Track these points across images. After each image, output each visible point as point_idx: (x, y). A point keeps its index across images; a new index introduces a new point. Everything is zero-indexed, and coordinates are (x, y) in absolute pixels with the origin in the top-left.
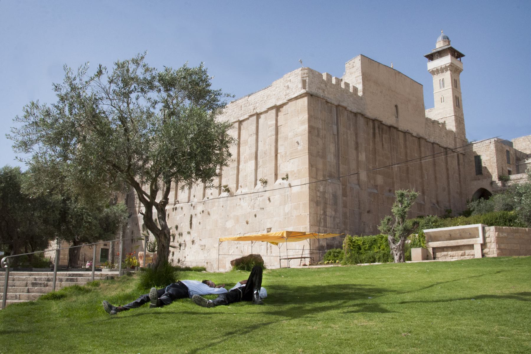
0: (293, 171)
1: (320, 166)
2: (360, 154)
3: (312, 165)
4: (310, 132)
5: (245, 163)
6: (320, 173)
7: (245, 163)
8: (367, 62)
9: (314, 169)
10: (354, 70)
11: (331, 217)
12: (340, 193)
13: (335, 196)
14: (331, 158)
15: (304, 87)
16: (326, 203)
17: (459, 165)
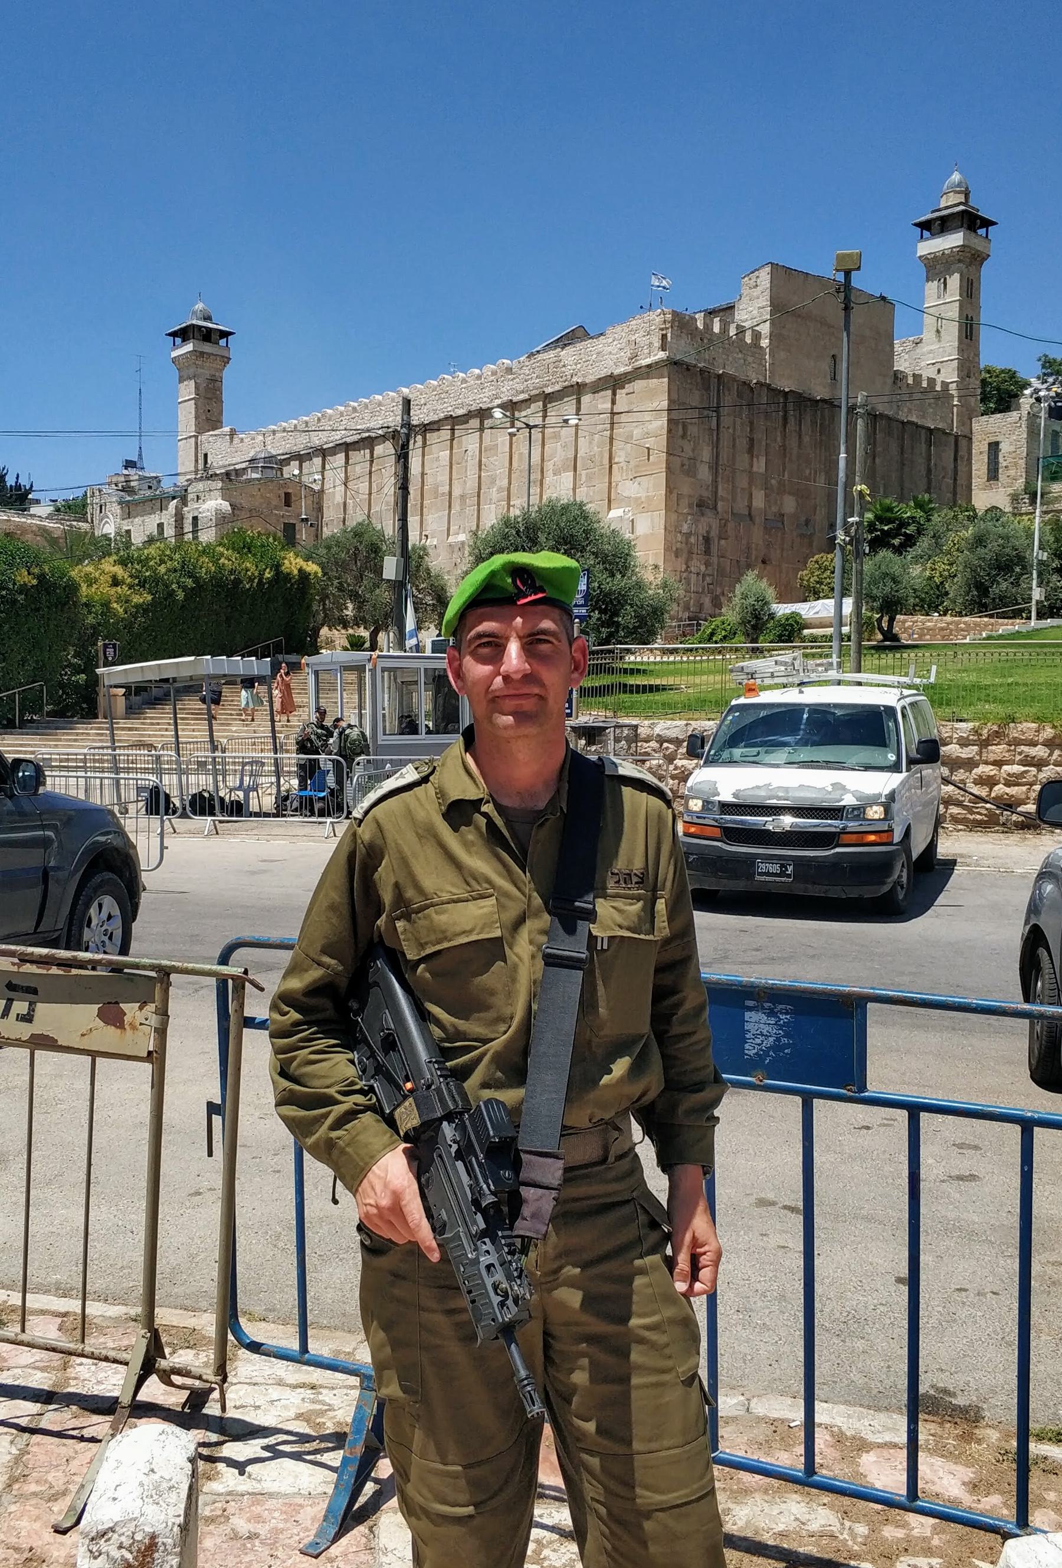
0: (640, 498)
1: (686, 490)
2: (755, 459)
3: (670, 489)
4: (669, 431)
5: (555, 474)
6: (685, 502)
7: (555, 474)
8: (783, 275)
9: (674, 496)
10: (756, 292)
11: (698, 574)
12: (714, 533)
13: (707, 540)
14: (704, 473)
15: (663, 348)
16: (690, 553)
17: (956, 460)
